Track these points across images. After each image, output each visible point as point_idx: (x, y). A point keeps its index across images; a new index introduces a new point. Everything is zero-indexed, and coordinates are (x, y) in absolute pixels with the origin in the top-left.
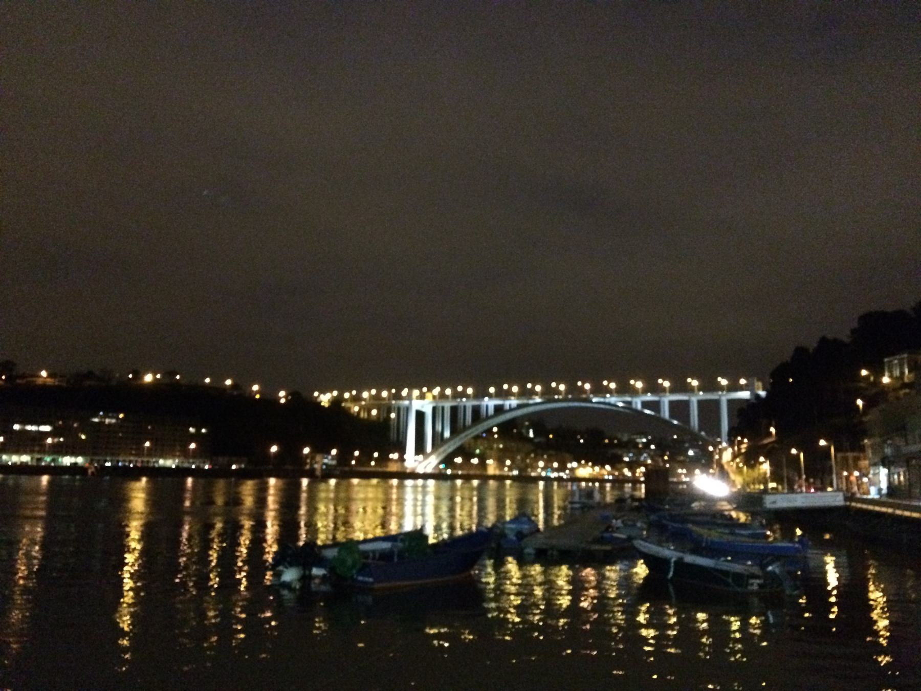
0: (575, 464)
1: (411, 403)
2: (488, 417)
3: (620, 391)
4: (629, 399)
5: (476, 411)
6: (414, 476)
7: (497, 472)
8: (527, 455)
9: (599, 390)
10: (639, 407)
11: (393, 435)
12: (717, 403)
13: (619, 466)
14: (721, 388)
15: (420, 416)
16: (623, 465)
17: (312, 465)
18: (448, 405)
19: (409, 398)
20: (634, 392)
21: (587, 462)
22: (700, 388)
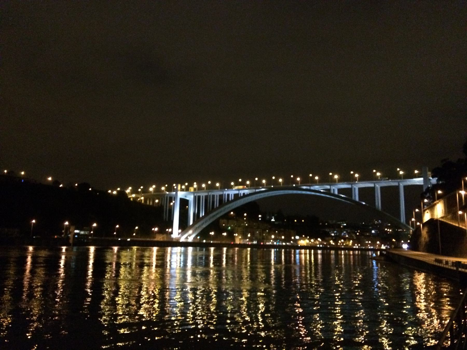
0: (297, 237)
1: (177, 193)
2: (229, 202)
3: (322, 181)
4: (328, 187)
5: (221, 196)
6: (176, 244)
7: (242, 242)
8: (264, 230)
9: (308, 181)
10: (336, 193)
11: (165, 216)
12: (397, 188)
13: (327, 239)
14: (399, 177)
15: (184, 203)
16: (330, 238)
17: (66, 234)
18: (203, 194)
19: (176, 191)
20: (332, 182)
21: (306, 236)
22: (382, 177)
